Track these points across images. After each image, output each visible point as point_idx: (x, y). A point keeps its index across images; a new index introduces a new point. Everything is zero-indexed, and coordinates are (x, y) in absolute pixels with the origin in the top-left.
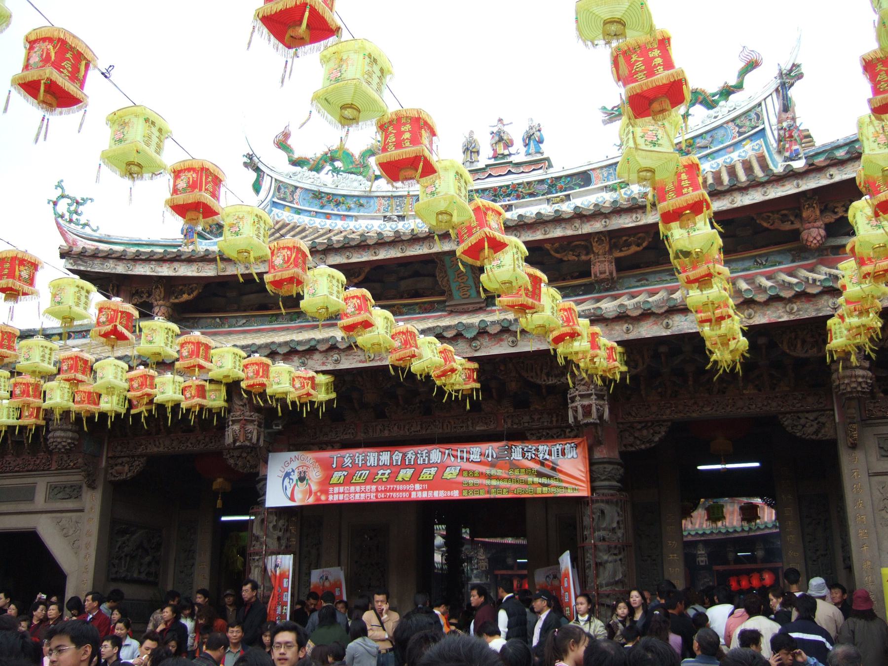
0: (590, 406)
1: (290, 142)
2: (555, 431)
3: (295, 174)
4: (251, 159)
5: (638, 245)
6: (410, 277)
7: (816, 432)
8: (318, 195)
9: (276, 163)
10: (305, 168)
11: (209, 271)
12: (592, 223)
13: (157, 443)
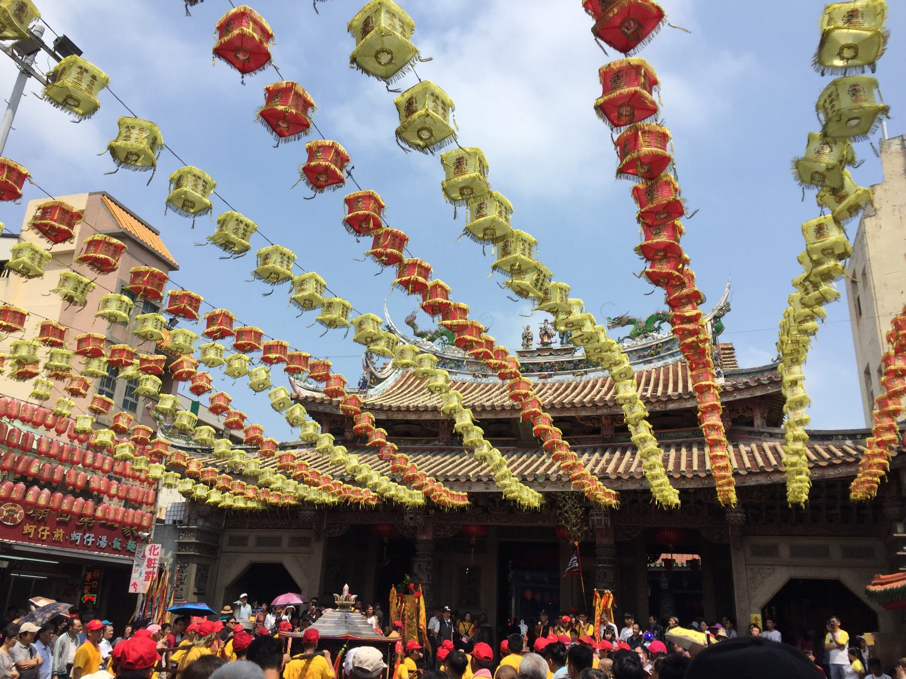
1: (416, 322)
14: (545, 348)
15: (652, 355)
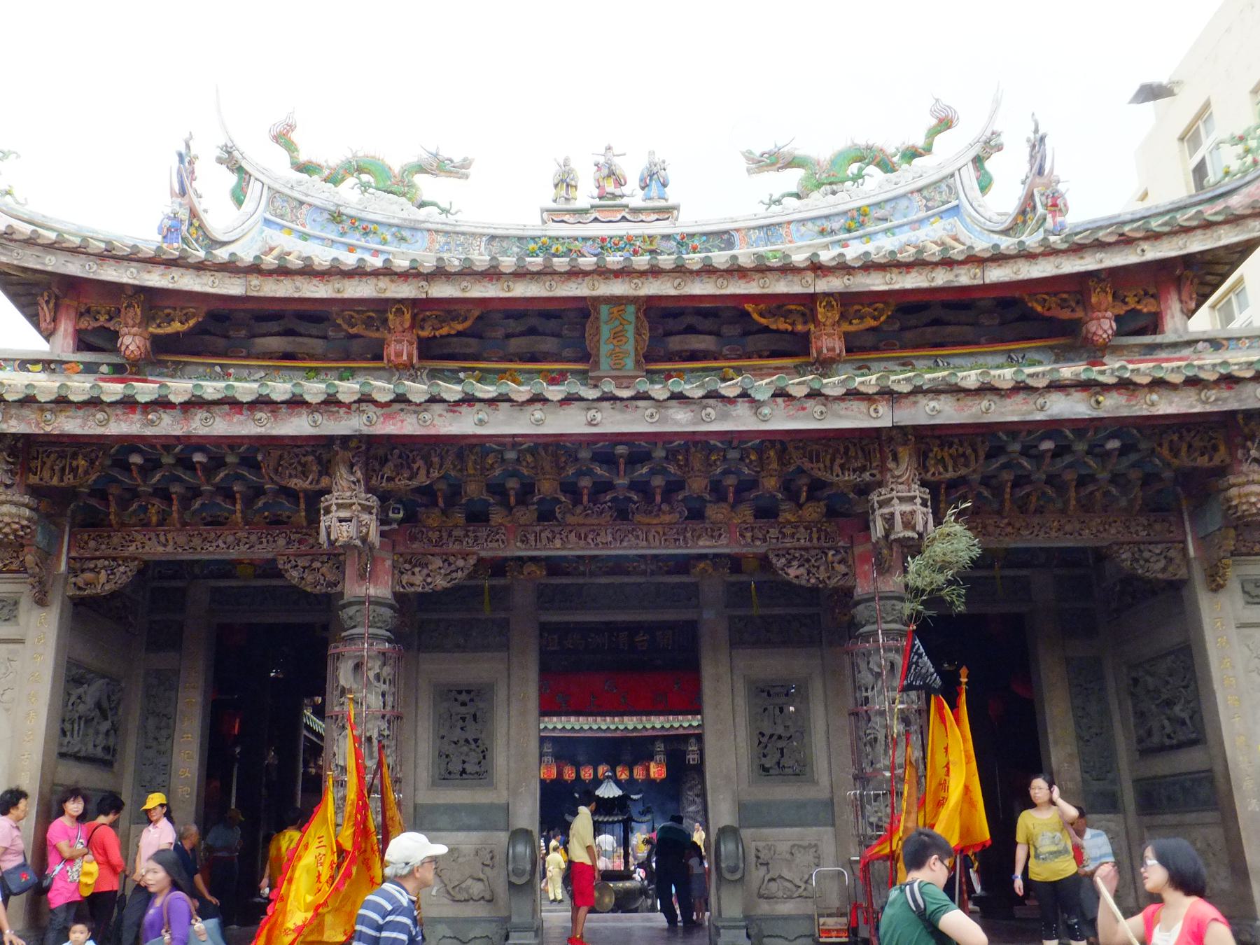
0: (913, 513)
1: (294, 136)
2: (813, 552)
3: (299, 183)
4: (229, 153)
5: (875, 318)
6: (522, 334)
7: (1164, 570)
8: (336, 217)
9: (271, 164)
10: (315, 177)
11: (233, 287)
12: (830, 278)
13: (162, 539)
14: (609, 204)
15: (849, 231)
